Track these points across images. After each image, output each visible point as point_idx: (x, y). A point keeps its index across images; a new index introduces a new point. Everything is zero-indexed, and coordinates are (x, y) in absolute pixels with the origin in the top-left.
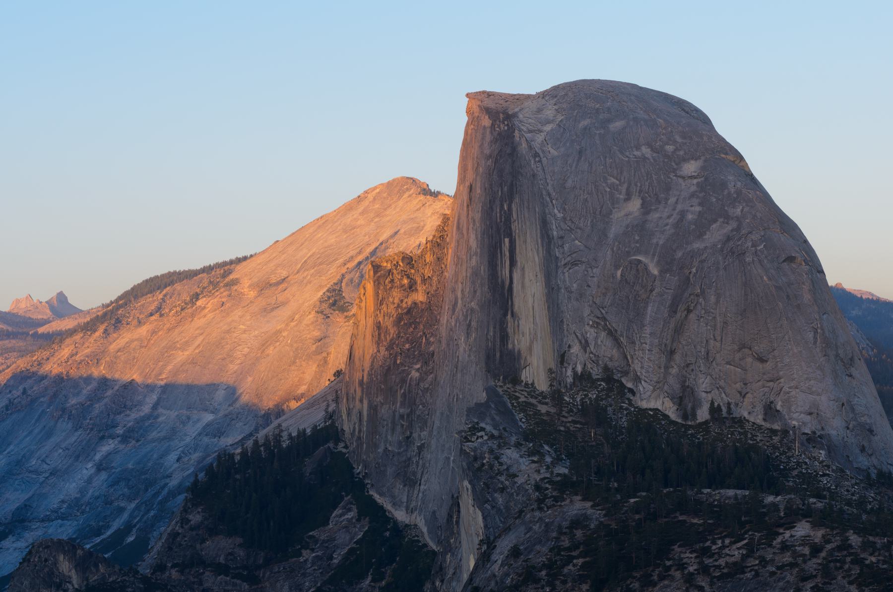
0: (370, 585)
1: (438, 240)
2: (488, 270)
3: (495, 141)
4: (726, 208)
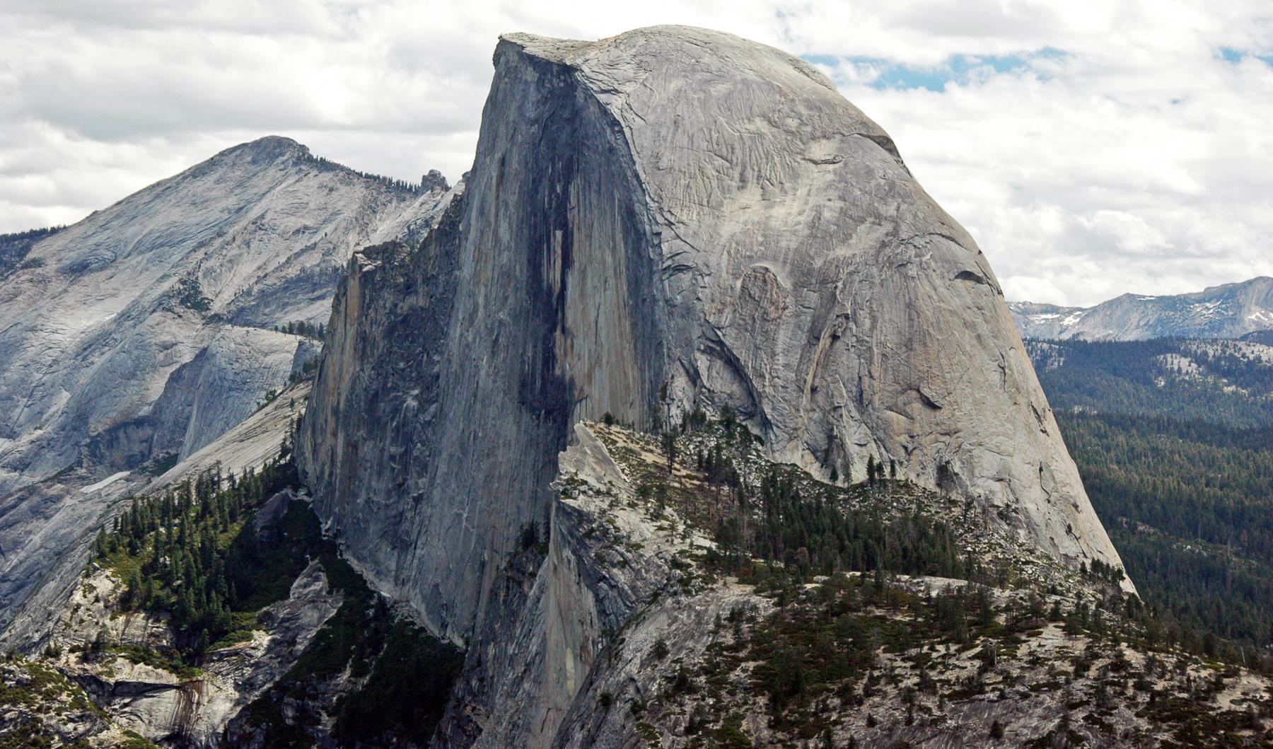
0: (349, 681)
1: (447, 228)
3: (544, 101)
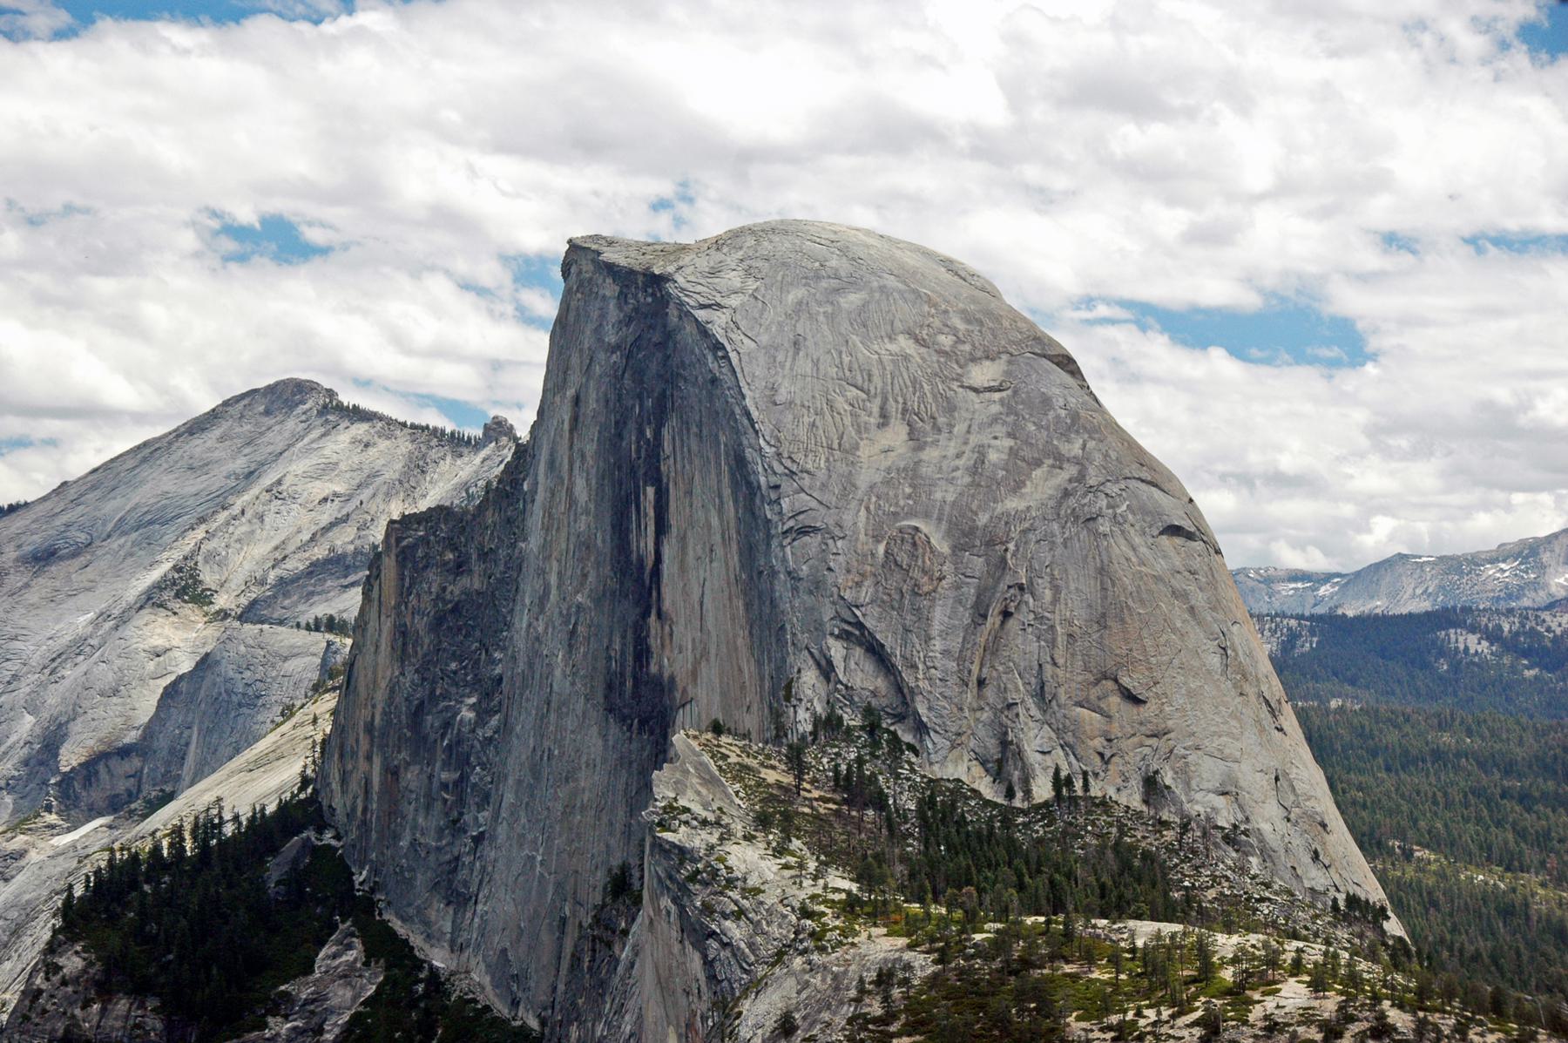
1: (508, 488)
2: (612, 540)
3: (628, 321)
4: (1055, 442)
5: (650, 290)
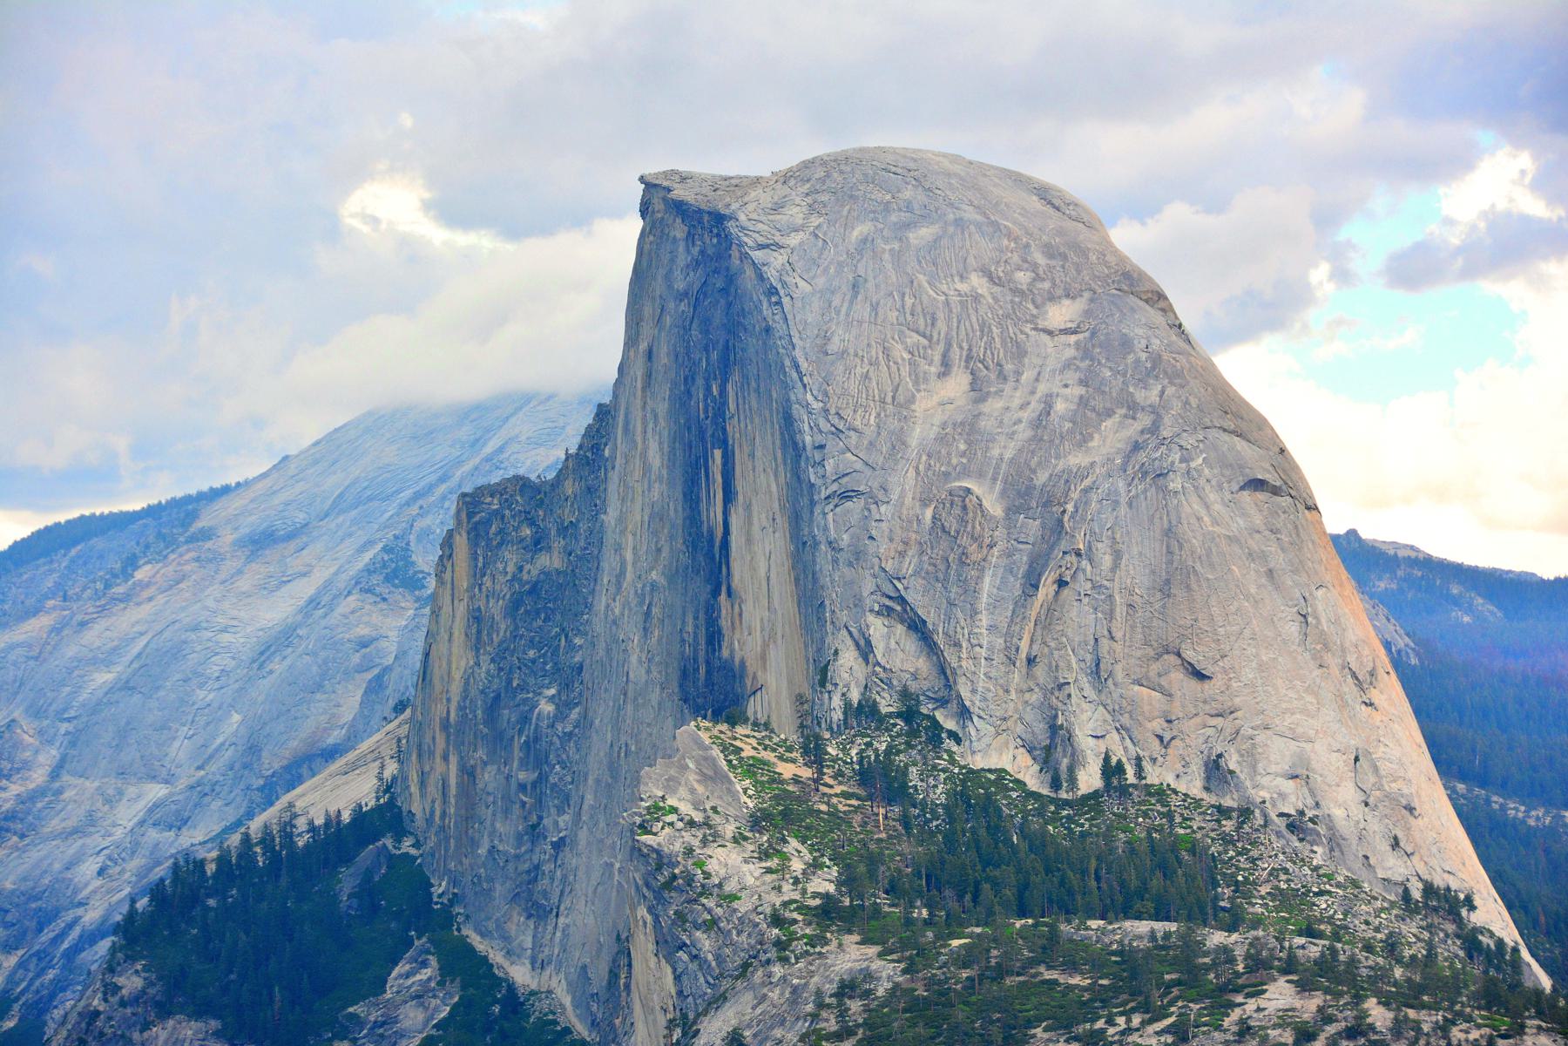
1: (589, 454)
2: (684, 509)
4: (1131, 390)
5: (715, 231)
